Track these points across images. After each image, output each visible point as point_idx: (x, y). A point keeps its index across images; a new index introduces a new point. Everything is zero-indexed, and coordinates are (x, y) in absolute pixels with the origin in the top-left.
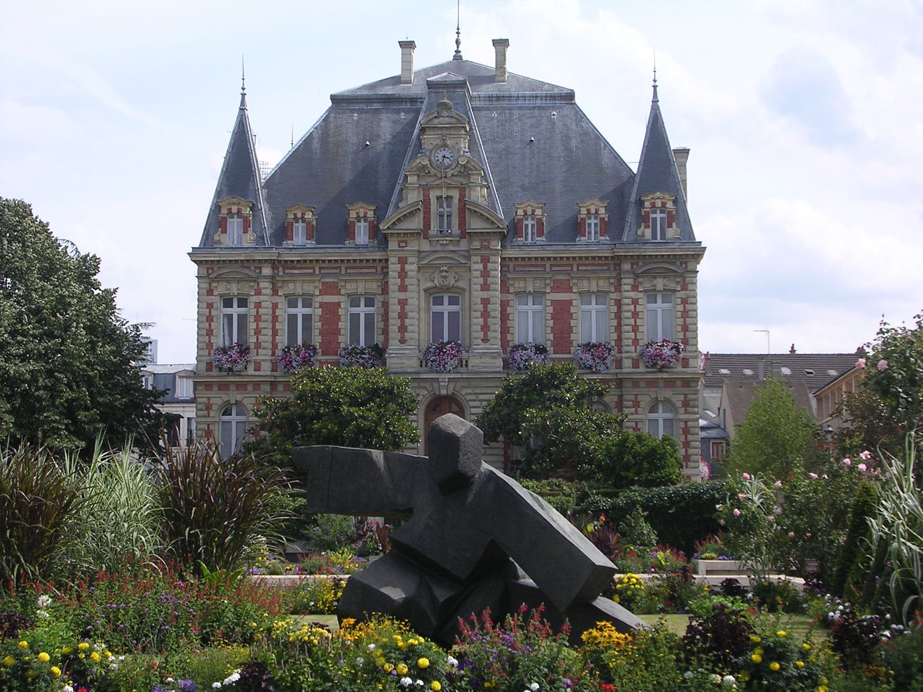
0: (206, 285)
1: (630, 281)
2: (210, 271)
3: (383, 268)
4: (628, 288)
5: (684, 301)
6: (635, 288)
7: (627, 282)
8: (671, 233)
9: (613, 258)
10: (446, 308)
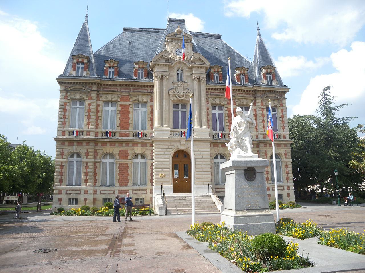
0: (64, 94)
1: (260, 101)
2: (67, 88)
3: (151, 90)
4: (260, 104)
5: (282, 111)
6: (262, 104)
7: (259, 101)
8: (274, 83)
9: (252, 91)
10: (180, 110)
